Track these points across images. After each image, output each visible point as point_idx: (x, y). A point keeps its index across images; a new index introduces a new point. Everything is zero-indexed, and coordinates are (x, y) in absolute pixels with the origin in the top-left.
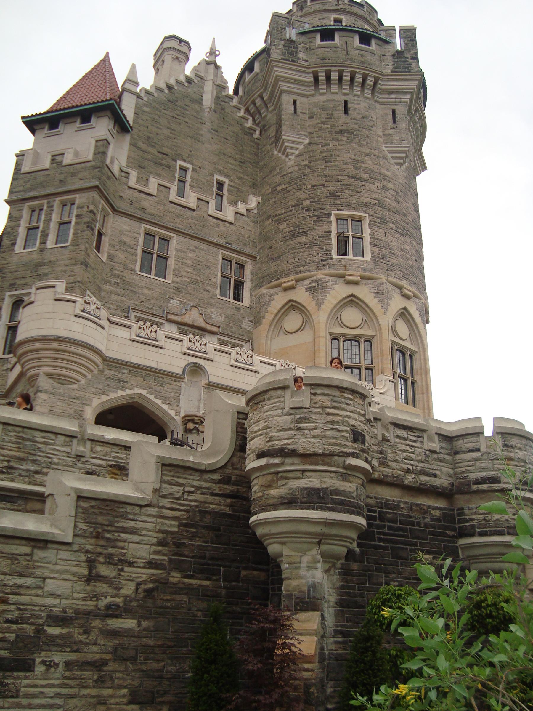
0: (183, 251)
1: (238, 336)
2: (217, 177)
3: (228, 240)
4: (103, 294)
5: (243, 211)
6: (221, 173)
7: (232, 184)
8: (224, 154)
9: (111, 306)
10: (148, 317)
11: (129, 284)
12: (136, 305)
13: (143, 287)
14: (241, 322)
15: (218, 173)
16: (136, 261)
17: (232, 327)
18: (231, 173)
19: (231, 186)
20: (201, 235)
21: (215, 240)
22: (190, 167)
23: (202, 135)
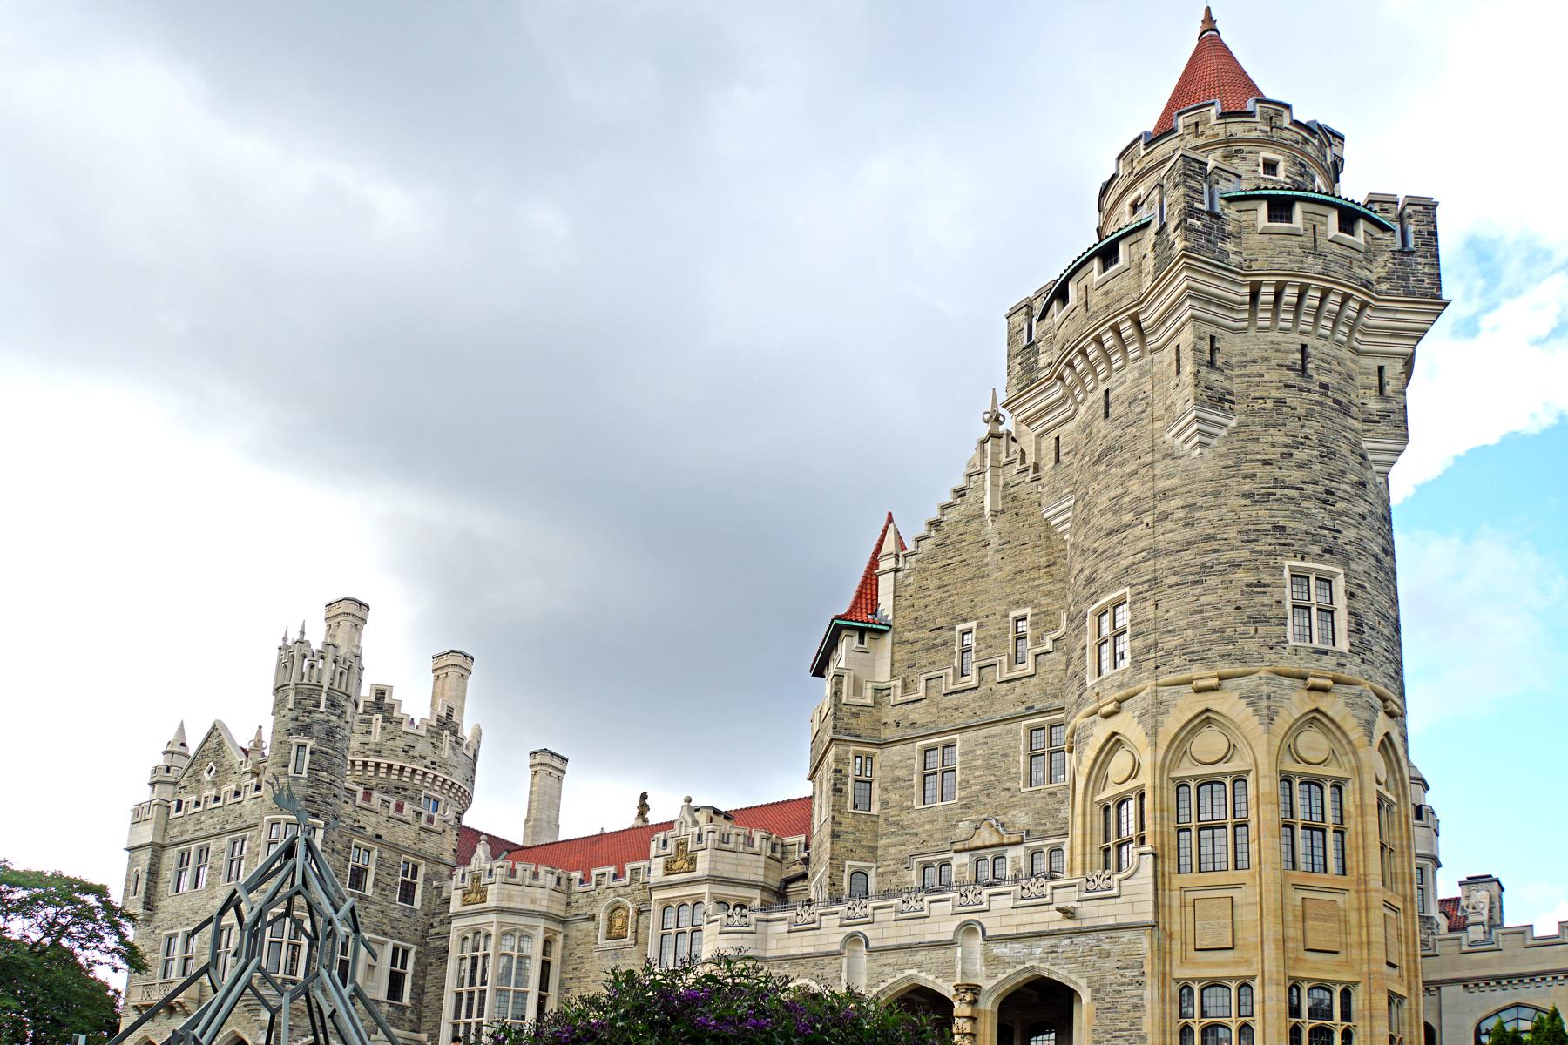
0: (973, 751)
1: (1055, 832)
2: (1013, 614)
3: (1029, 704)
4: (880, 852)
5: (1048, 646)
6: (1018, 604)
7: (1036, 611)
8: (1022, 571)
9: (891, 863)
10: (932, 858)
11: (909, 827)
12: (917, 848)
13: (923, 823)
14: (1058, 810)
15: (1014, 607)
16: (913, 794)
17: (1045, 824)
18: (1032, 595)
19: (1037, 614)
20: (989, 717)
21: (1012, 711)
22: (973, 624)
23: (987, 565)
